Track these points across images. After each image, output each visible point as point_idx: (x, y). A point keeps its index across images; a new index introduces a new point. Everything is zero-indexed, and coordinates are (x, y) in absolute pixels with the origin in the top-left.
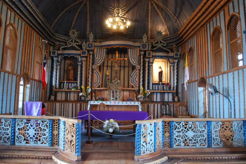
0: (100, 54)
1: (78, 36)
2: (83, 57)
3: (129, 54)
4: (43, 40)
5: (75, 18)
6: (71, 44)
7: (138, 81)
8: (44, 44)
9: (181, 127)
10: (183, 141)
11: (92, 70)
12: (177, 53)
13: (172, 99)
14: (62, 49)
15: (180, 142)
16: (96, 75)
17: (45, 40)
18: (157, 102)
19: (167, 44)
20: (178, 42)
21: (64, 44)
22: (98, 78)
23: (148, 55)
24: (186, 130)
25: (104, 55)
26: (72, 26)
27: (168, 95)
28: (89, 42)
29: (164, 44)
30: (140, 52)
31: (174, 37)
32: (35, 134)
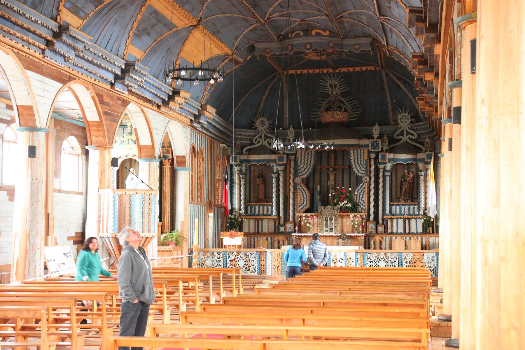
0: (306, 159)
2: (279, 165)
3: (352, 158)
5: (264, 97)
6: (259, 142)
7: (366, 202)
11: (295, 184)
14: (246, 151)
17: (224, 145)
18: (397, 234)
21: (249, 142)
22: (303, 197)
23: (382, 159)
24: (378, 260)
25: (312, 161)
26: (260, 110)
29: (412, 135)
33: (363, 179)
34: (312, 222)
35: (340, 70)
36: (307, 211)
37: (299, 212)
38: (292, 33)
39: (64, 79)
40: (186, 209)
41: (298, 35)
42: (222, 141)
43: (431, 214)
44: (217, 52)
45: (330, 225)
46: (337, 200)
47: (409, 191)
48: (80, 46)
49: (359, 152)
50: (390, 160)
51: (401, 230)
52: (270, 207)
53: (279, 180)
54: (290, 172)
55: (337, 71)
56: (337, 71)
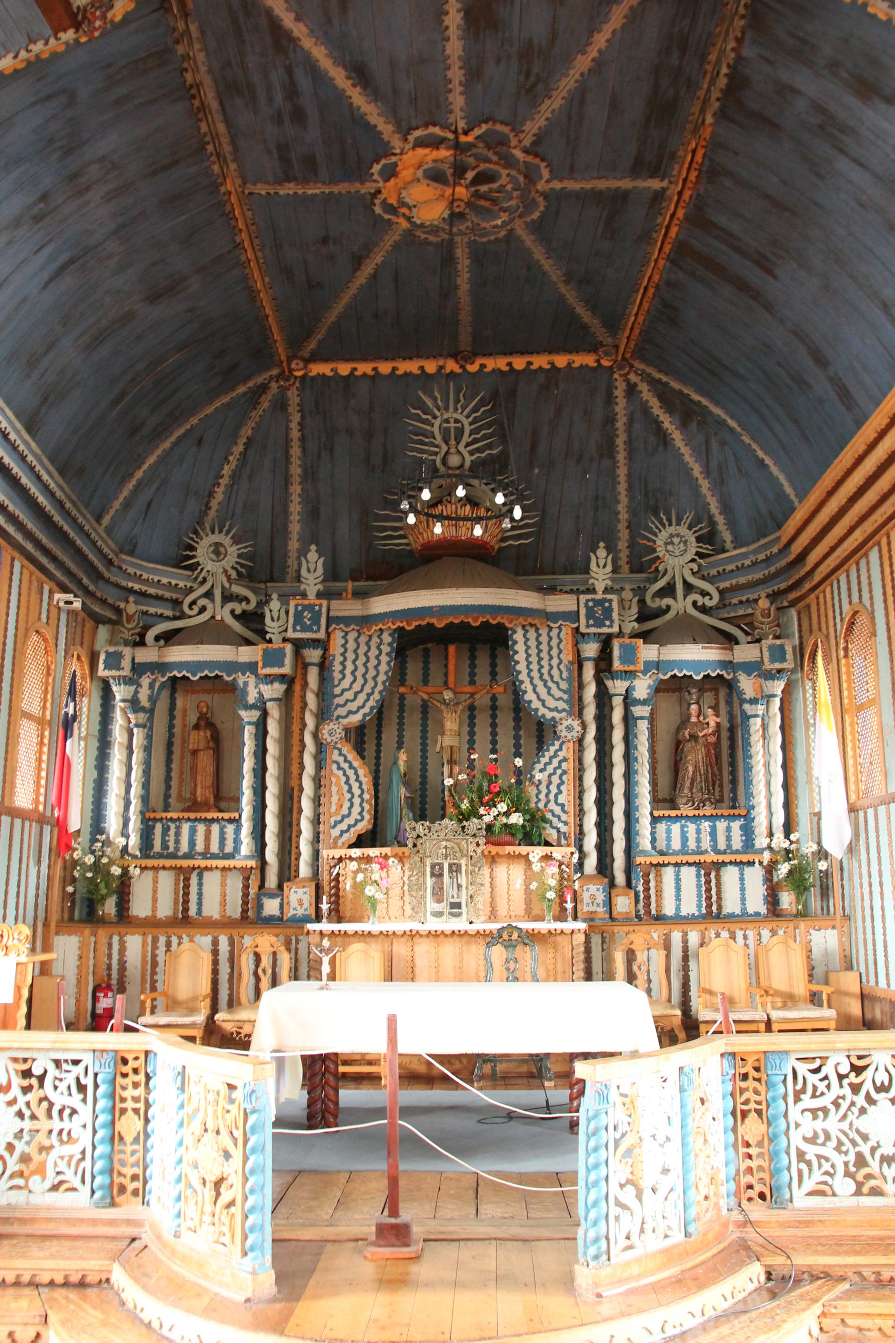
1: (242, 566)
2: (270, 679)
3: (521, 657)
4: (57, 596)
5: (227, 470)
6: (203, 610)
7: (570, 808)
8: (63, 617)
9: (828, 1087)
10: (846, 1164)
11: (321, 747)
12: (778, 642)
13: (768, 903)
14: (157, 638)
15: (826, 1173)
16: (344, 779)
17: (70, 597)
18: (679, 920)
19: (722, 598)
20: (783, 586)
22: (350, 790)
24: (860, 1100)
25: (383, 667)
26: (212, 513)
27: (742, 874)
28: (299, 600)
29: (704, 594)
30: (576, 644)
31: (762, 557)
32: (19, 1135)
33: (561, 729)
35: (483, 366)
36: (360, 842)
37: (335, 846)
42: (65, 580)
45: (450, 891)
46: (472, 801)
49: (544, 639)
51: (690, 906)
52: (230, 829)
53: (265, 733)
54: (304, 705)
55: (473, 368)
56: (473, 368)
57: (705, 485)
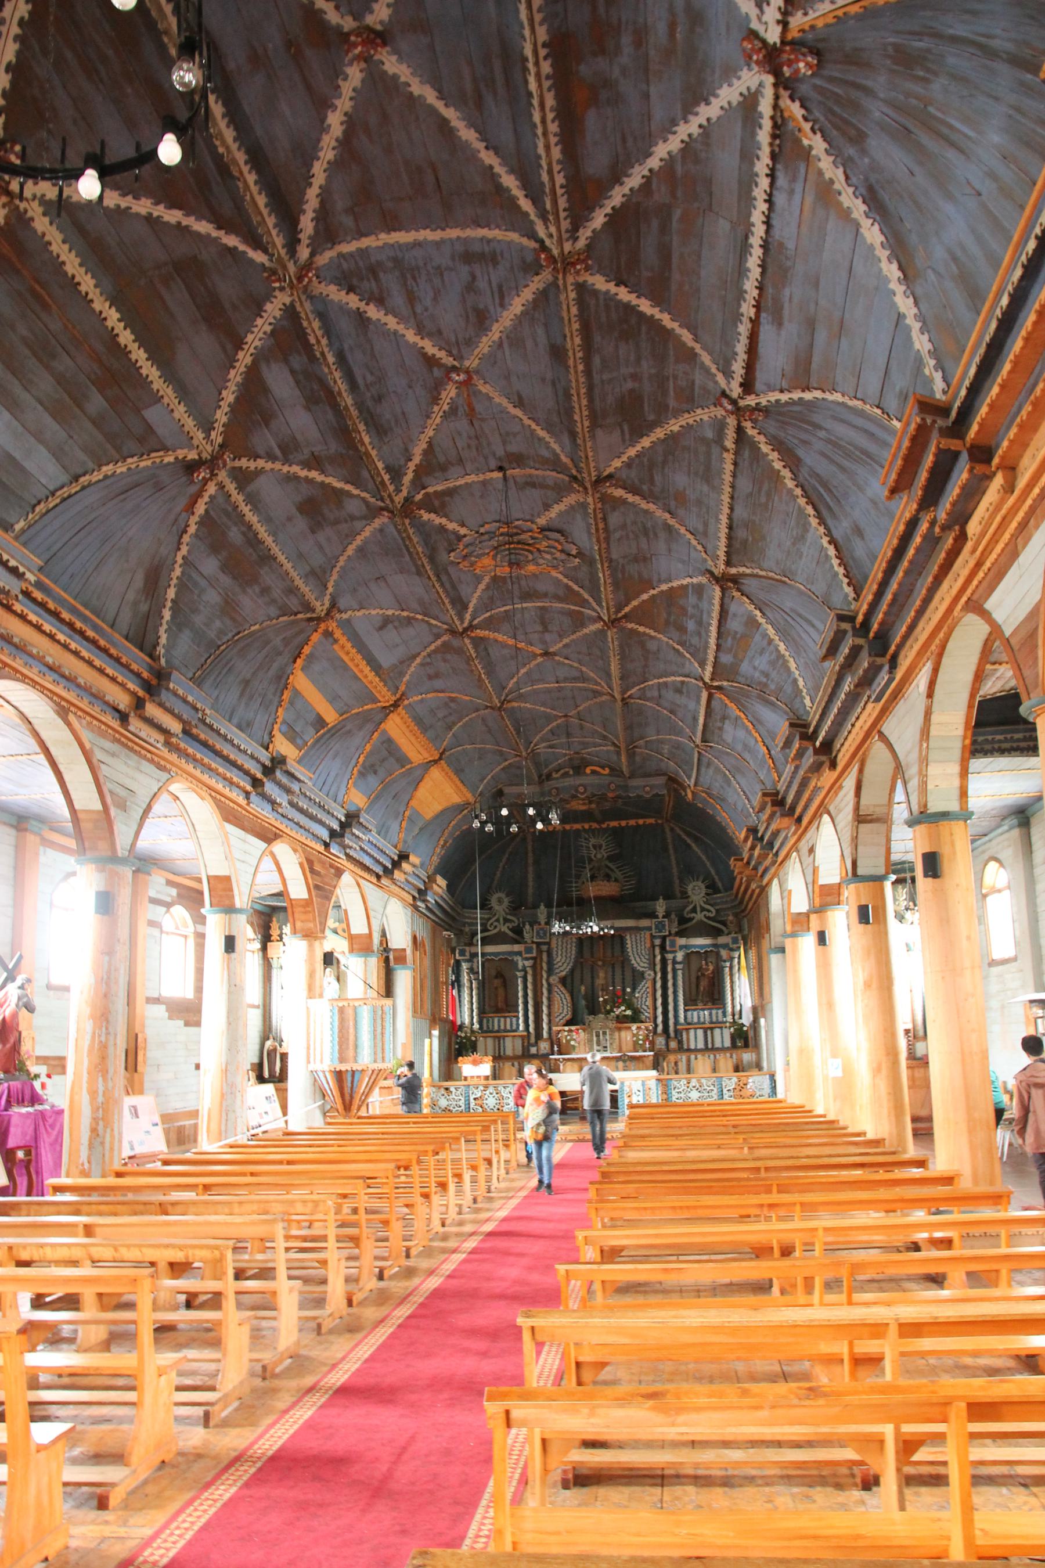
2: (527, 959)
11: (549, 985)
18: (696, 1050)
34: (577, 1037)
36: (568, 1023)
38: (557, 771)
39: (269, 836)
40: (408, 1026)
41: (566, 775)
43: (747, 1020)
44: (456, 799)
45: (603, 1042)
47: (710, 990)
48: (295, 787)
50: (681, 947)
51: (701, 1045)
55: (604, 826)
56: (604, 826)
57: (708, 864)
